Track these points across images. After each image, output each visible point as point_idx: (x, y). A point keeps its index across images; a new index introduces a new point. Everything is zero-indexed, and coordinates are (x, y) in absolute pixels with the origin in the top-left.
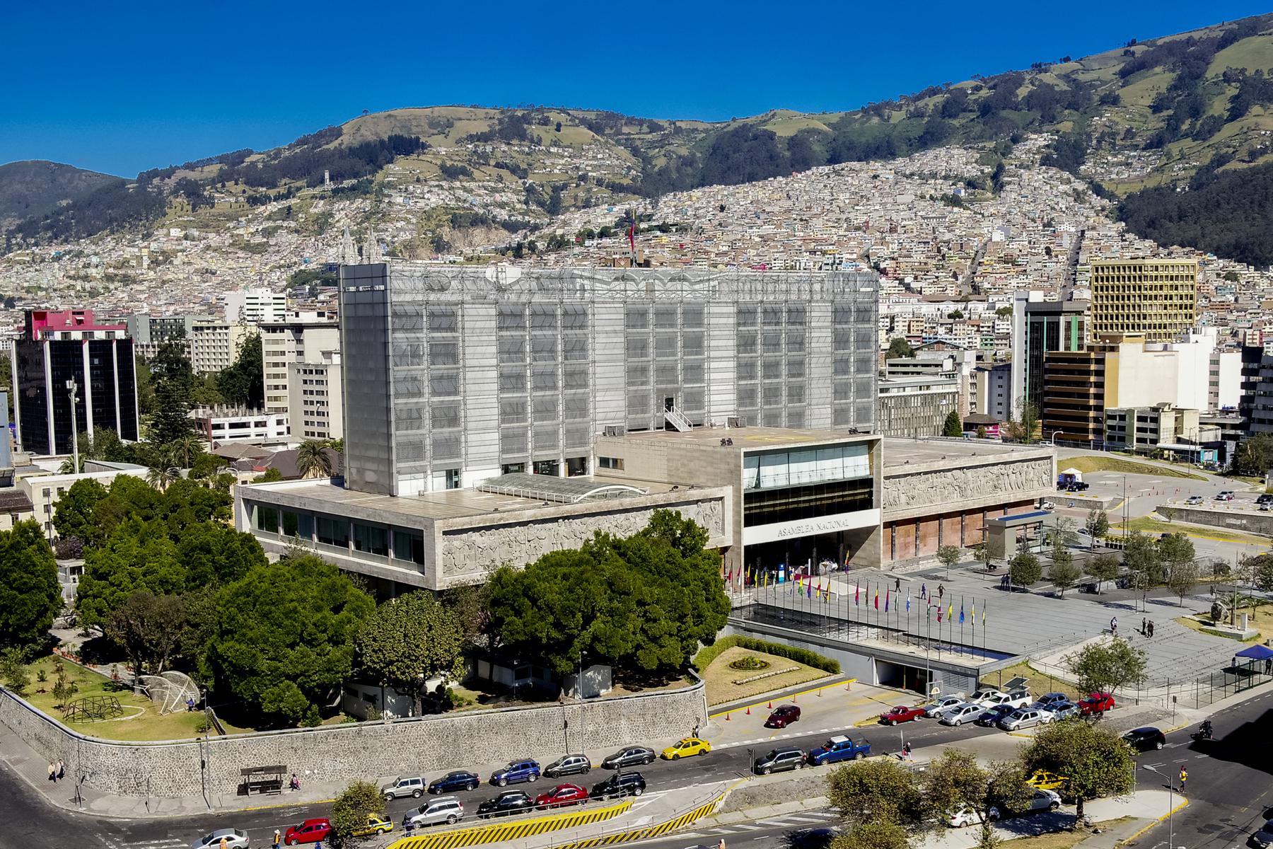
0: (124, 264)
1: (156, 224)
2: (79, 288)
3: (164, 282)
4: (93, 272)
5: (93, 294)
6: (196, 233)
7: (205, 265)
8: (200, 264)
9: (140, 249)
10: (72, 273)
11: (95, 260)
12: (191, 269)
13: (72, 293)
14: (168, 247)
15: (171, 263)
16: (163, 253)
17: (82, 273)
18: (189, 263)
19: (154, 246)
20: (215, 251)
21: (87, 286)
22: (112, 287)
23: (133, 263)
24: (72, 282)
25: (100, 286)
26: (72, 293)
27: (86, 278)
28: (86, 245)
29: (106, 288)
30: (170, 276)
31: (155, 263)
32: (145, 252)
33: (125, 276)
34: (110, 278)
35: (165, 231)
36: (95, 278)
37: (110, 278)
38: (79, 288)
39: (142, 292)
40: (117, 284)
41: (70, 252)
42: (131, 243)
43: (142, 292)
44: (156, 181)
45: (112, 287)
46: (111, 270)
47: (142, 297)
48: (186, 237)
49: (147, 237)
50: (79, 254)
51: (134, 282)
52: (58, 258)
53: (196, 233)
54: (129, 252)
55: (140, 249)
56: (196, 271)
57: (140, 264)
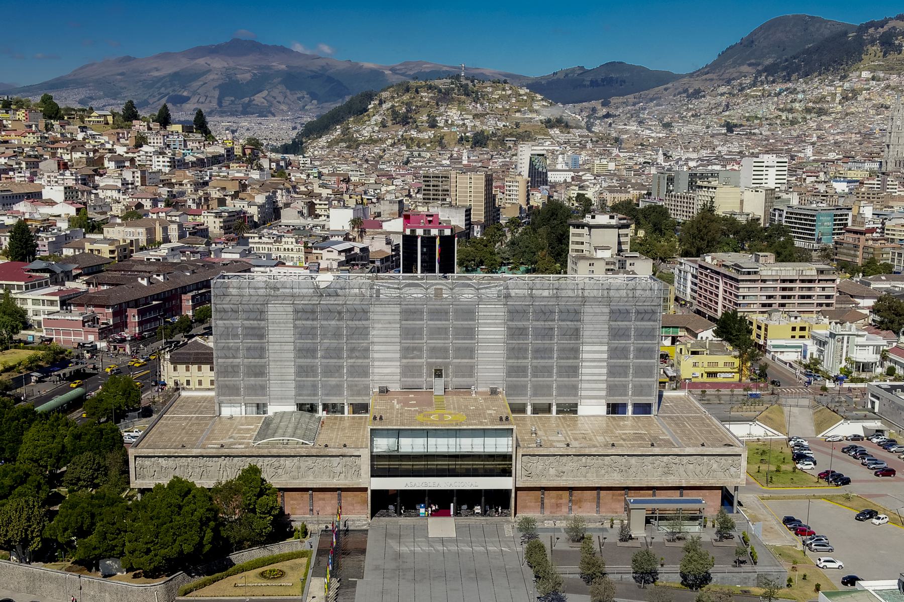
0: (822, 99)
1: (853, 68)
2: (784, 118)
3: (847, 114)
4: (797, 105)
5: (793, 122)
6: (882, 75)
7: (881, 101)
8: (879, 100)
9: (836, 88)
10: (782, 106)
11: (800, 96)
12: (870, 104)
13: (778, 122)
14: (858, 86)
15: (856, 99)
16: (853, 91)
17: (789, 106)
18: (870, 100)
19: (847, 85)
20: (893, 89)
21: (790, 116)
22: (808, 117)
23: (829, 99)
24: (780, 113)
25: (799, 116)
26: (778, 122)
27: (791, 110)
28: (801, 85)
29: (804, 119)
30: (853, 110)
31: (845, 98)
32: (839, 90)
33: (820, 109)
34: (808, 110)
35: (858, 73)
36: (798, 110)
37: (808, 110)
38: (784, 118)
39: (828, 122)
40: (813, 115)
41: (787, 89)
42: (831, 84)
43: (828, 122)
44: (871, 31)
45: (808, 117)
46: (811, 104)
47: (827, 126)
48: (873, 79)
49: (843, 78)
50: (794, 91)
51: (825, 114)
52: (778, 95)
53: (882, 75)
54: (826, 90)
55: (836, 88)
56: (874, 106)
57: (834, 100)
